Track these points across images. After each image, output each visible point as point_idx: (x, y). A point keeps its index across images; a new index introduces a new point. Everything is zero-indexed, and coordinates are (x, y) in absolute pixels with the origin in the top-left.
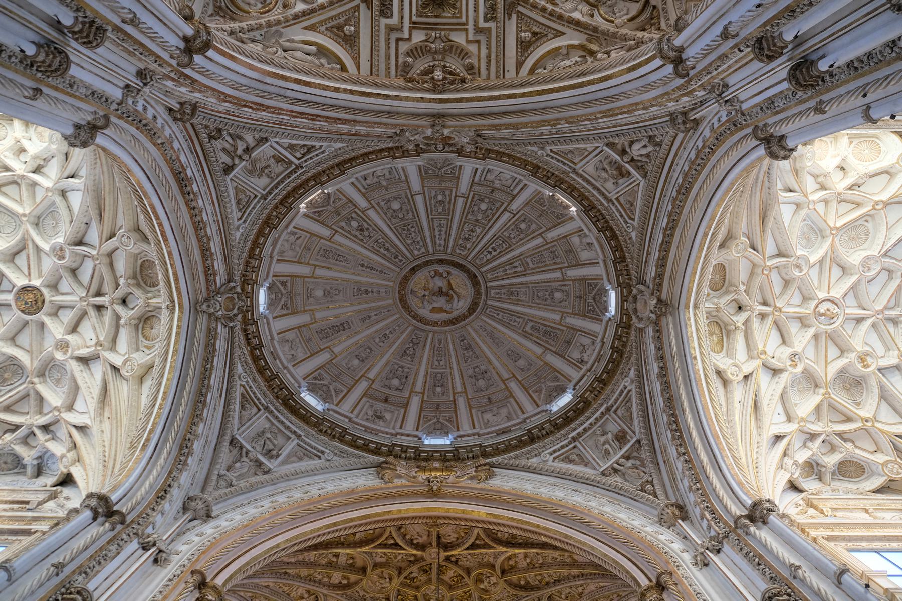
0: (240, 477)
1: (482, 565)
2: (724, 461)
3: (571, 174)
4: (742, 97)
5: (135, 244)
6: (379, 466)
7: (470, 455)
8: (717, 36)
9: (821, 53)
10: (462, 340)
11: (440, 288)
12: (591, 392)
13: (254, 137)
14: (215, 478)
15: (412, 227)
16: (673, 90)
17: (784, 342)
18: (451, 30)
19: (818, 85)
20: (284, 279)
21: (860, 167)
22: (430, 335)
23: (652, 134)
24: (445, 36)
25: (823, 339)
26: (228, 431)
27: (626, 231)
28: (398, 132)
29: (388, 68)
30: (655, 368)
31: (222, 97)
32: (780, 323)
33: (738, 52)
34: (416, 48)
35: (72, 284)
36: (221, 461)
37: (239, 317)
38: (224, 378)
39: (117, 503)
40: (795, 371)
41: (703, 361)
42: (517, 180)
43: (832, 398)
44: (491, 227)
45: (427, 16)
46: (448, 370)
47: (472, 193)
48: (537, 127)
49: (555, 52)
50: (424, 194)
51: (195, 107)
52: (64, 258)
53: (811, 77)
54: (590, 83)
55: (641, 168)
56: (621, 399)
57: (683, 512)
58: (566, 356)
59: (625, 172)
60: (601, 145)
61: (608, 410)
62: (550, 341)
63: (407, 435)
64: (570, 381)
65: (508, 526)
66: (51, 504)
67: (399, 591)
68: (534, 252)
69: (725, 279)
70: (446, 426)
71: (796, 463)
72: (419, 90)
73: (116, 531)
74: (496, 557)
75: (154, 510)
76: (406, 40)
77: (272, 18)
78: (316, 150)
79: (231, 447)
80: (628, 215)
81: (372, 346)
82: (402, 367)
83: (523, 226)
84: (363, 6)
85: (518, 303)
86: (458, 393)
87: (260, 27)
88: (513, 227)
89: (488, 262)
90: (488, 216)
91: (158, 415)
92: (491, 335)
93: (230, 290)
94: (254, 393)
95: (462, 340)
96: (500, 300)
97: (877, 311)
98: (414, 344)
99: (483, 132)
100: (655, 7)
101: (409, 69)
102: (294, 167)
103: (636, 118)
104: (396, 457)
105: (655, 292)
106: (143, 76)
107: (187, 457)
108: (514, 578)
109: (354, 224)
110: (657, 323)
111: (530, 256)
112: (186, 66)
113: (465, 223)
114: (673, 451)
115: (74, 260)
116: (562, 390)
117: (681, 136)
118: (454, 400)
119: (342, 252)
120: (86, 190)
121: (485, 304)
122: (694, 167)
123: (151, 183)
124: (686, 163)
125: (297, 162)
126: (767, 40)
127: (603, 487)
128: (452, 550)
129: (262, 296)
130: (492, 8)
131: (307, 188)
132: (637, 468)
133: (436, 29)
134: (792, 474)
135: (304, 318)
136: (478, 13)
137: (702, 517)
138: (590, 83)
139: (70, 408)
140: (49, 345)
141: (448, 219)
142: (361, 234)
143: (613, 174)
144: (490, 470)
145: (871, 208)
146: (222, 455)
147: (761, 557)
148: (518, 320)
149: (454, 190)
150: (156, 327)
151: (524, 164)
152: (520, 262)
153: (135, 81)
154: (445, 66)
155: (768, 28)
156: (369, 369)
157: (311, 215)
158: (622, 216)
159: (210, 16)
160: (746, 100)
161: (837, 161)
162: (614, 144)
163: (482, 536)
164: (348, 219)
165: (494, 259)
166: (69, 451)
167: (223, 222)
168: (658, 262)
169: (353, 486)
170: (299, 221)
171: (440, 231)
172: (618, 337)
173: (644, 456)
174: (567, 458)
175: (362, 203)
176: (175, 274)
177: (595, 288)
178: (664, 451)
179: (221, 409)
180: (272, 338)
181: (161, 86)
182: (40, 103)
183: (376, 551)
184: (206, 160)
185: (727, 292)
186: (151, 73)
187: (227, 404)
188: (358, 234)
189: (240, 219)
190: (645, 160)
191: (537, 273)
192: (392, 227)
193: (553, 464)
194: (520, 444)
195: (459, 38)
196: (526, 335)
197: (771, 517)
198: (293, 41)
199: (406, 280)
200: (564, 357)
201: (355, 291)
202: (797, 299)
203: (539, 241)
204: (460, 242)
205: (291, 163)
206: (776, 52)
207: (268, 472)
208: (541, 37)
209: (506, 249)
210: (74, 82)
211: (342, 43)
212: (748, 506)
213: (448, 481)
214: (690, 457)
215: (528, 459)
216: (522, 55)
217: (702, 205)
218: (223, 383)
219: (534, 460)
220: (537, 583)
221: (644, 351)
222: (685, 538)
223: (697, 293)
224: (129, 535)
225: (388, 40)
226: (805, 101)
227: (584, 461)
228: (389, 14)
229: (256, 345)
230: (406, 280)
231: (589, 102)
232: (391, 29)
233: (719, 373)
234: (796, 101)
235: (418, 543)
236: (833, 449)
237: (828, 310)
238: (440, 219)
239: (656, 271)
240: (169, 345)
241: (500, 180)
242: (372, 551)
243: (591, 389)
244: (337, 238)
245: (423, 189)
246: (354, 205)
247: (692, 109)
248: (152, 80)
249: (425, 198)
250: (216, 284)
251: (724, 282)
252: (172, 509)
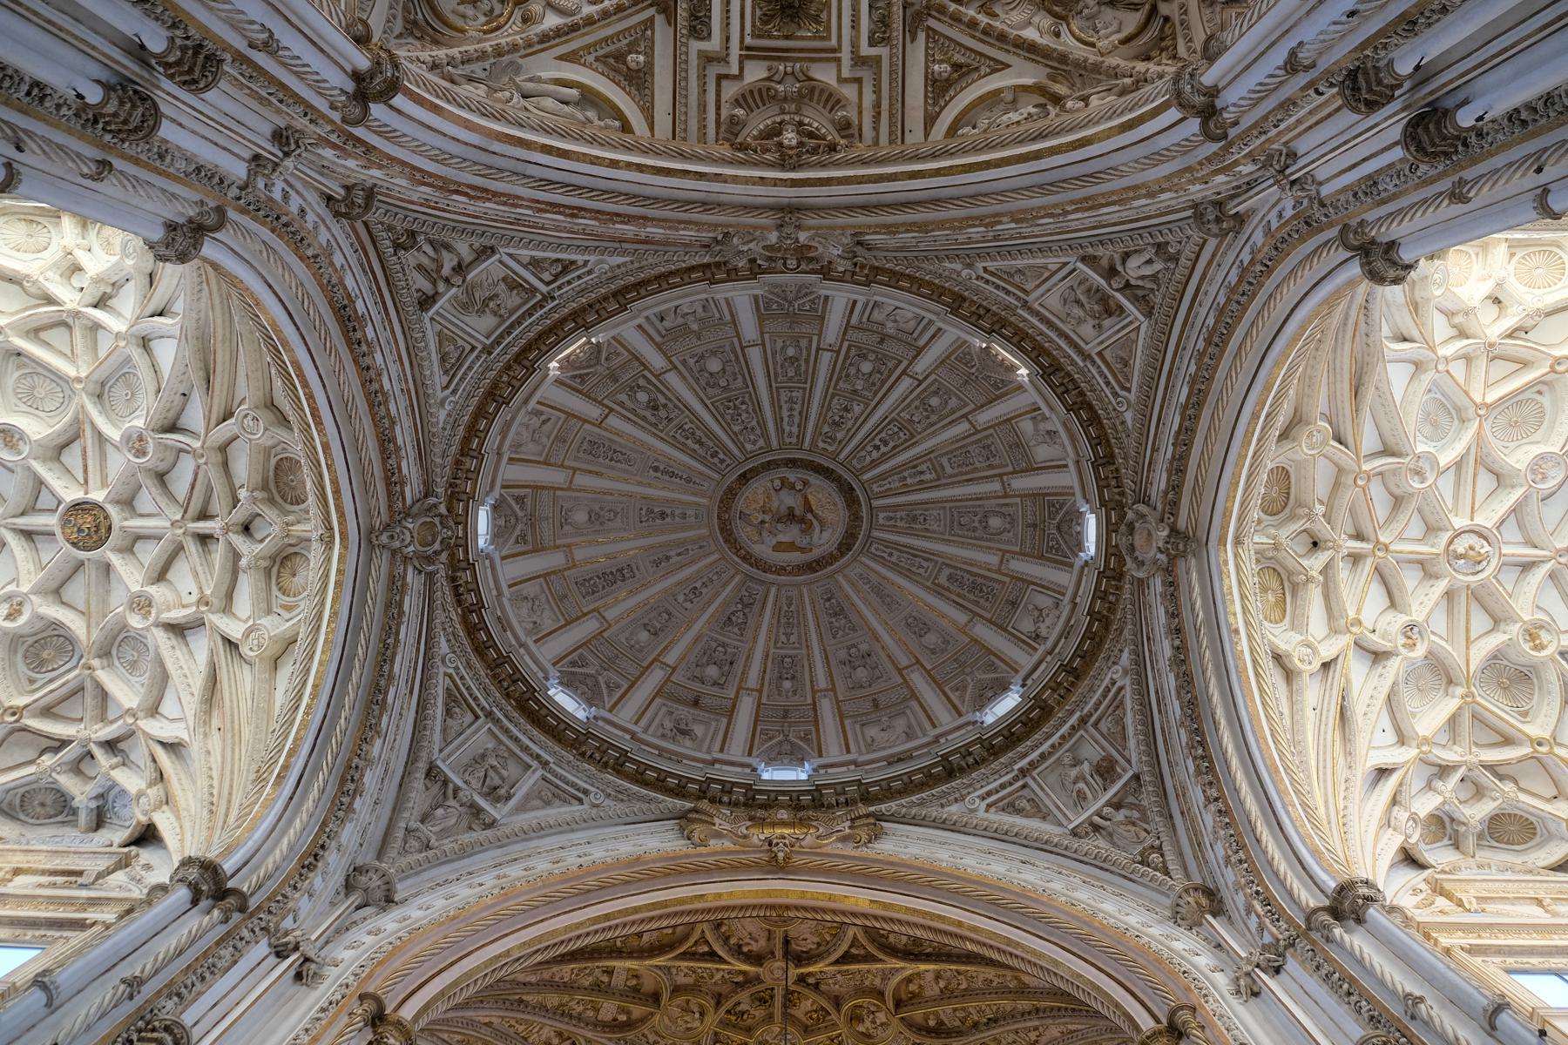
0: (444, 833)
1: (861, 991)
2: (1287, 813)
3: (1019, 311)
4: (1321, 175)
5: (266, 429)
6: (683, 817)
7: (842, 799)
8: (1279, 68)
9: (1461, 96)
10: (829, 600)
11: (791, 509)
12: (1054, 690)
13: (471, 246)
14: (400, 834)
15: (743, 403)
16: (1200, 163)
17: (1393, 604)
19: (1457, 151)
20: (522, 492)
21: (1528, 297)
22: (773, 590)
23: (1162, 240)
24: (802, 71)
25: (1462, 599)
26: (424, 754)
27: (1115, 410)
28: (720, 238)
29: (703, 127)
30: (1165, 648)
31: (418, 176)
32: (1386, 571)
33: (1314, 95)
34: (751, 92)
35: (158, 499)
36: (411, 805)
37: (444, 556)
38: (416, 662)
39: (233, 876)
40: (1412, 655)
41: (1250, 637)
42: (925, 322)
43: (1479, 704)
44: (879, 403)
45: (770, 37)
46: (804, 651)
47: (846, 344)
48: (960, 228)
50: (763, 344)
51: (371, 193)
52: (144, 454)
53: (1445, 138)
54: (1053, 151)
55: (1143, 301)
57: (1214, 901)
58: (1009, 628)
59: (1114, 307)
60: (1072, 259)
61: (1083, 721)
62: (982, 601)
63: (732, 764)
64: (1017, 671)
65: (908, 923)
66: (119, 877)
67: (716, 1034)
68: (954, 447)
69: (1288, 493)
70: (800, 748)
71: (1413, 818)
72: (756, 164)
73: (231, 923)
74: (886, 976)
75: (295, 888)
76: (735, 77)
77: (503, 41)
78: (578, 268)
79: (427, 781)
80: (1118, 381)
81: (672, 610)
82: (724, 645)
83: (935, 401)
84: (660, 20)
85: (926, 534)
86: (821, 691)
87: (483, 56)
88: (917, 403)
89: (875, 464)
90: (874, 384)
91: (304, 725)
92: (878, 590)
93: (429, 510)
94: (468, 688)
95: (829, 600)
96: (894, 529)
97: (1558, 551)
98: (745, 606)
99: (867, 237)
100: (1167, 19)
101: (739, 128)
102: (539, 297)
103: (1134, 211)
104: (712, 801)
105: (1167, 515)
106: (284, 140)
107: (354, 798)
108: (917, 1014)
109: (642, 397)
110: (1169, 570)
111: (947, 453)
112: (356, 123)
113: (833, 395)
114: (1196, 795)
115: (161, 456)
116: (1002, 688)
117: (1212, 243)
118: (814, 704)
119: (620, 445)
120: (184, 336)
121: (869, 536)
122: (1236, 297)
123: (295, 324)
124: (1222, 291)
125: (544, 289)
126: (1366, 73)
127: (1075, 856)
128: (809, 965)
129: (483, 520)
130: (883, 22)
131: (562, 335)
132: (1134, 824)
133: (786, 59)
134: (1408, 837)
136: (858, 32)
137: (1249, 910)
138: (1053, 151)
139: (154, 711)
140: (118, 602)
141: (805, 389)
142: (654, 415)
143: (1092, 310)
144: (876, 826)
145: (1548, 369)
146: (413, 795)
147: (1352, 981)
148: (925, 564)
149: (815, 338)
150: (302, 573)
151: (937, 293)
152: (929, 464)
153: (270, 150)
154: (801, 124)
155: (1367, 52)
156: (666, 647)
157: (569, 381)
158: (1108, 383)
159: (396, 38)
160: (1328, 180)
161: (1487, 288)
162: (1095, 257)
163: (862, 939)
164: (632, 389)
165: (885, 458)
166: (150, 785)
167: (416, 393)
168: (1171, 463)
169: (639, 850)
170: (550, 392)
171: (791, 409)
172: (1100, 594)
173: (1145, 803)
174: (1011, 804)
175: (656, 360)
176: (335, 482)
177: (1061, 508)
178: (1182, 793)
180: (500, 594)
181: (313, 158)
182: (109, 187)
183: (678, 963)
184: (388, 285)
185: (1293, 517)
186: (297, 135)
187: (422, 706)
188: (648, 414)
189: (447, 387)
190: (1149, 285)
191: (959, 482)
192: (708, 402)
193: (986, 815)
194: (929, 780)
195: (825, 75)
196: (939, 590)
197: (1371, 910)
198: (539, 80)
199: (730, 495)
200: (1005, 630)
201: (643, 512)
202: (1416, 530)
203: (963, 427)
204: (826, 429)
205: (534, 290)
206: (1381, 95)
207: (492, 824)
208: (969, 73)
209: (906, 441)
210: (166, 151)
211: (624, 83)
212: (1329, 892)
213: (803, 843)
214: (1227, 804)
215: (942, 806)
216: (935, 104)
217: (1250, 364)
218: (415, 670)
219: (954, 808)
220: (958, 1023)
221: (1146, 618)
222: (1219, 946)
223: (1240, 519)
224: (254, 932)
225: (702, 78)
226: (1432, 181)
227: (1040, 811)
228: (705, 34)
229: (473, 604)
230: (730, 495)
231: (1051, 184)
232: (707, 59)
233: (1278, 658)
234: (1417, 180)
235: (750, 951)
236: (1479, 792)
237: (1472, 548)
238: (791, 389)
239: (1168, 480)
240: (323, 603)
241: (895, 321)
242: (669, 964)
243: (1054, 685)
244: (613, 421)
245: (762, 337)
246: (643, 364)
247: (1233, 197)
248: (298, 147)
249: (765, 351)
250: (404, 499)
251: (1288, 498)
252: (326, 887)
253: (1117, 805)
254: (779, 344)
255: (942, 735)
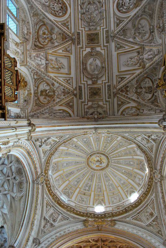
11: (98, 160)
14: (41, 231)
18: (99, 101)
26: (43, 216)
29: (82, 113)
30: (161, 195)
49: (128, 108)
55: (154, 140)
56: (151, 202)
61: (147, 205)
83: (121, 144)
84: (74, 97)
85: (120, 164)
89: (111, 153)
100: (156, 96)
104: (88, 217)
107: (33, 227)
110: (161, 182)
125: (58, 140)
132: (156, 225)
135: (61, 172)
149: (101, 136)
154: (97, 111)
158: (149, 151)
165: (113, 152)
166: (3, 220)
174: (136, 219)
179: (41, 209)
187: (43, 207)
188: (75, 147)
195: (101, 103)
196: (123, 173)
198: (56, 110)
199: (88, 158)
200: (134, 181)
203: (125, 148)
205: (56, 141)
211: (69, 108)
219: (128, 219)
230: (88, 158)
232: (82, 102)
243: (142, 196)
253: (153, 221)
254: (95, 136)
255: (125, 202)
